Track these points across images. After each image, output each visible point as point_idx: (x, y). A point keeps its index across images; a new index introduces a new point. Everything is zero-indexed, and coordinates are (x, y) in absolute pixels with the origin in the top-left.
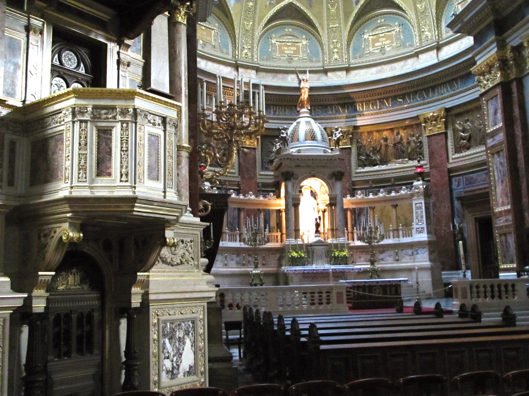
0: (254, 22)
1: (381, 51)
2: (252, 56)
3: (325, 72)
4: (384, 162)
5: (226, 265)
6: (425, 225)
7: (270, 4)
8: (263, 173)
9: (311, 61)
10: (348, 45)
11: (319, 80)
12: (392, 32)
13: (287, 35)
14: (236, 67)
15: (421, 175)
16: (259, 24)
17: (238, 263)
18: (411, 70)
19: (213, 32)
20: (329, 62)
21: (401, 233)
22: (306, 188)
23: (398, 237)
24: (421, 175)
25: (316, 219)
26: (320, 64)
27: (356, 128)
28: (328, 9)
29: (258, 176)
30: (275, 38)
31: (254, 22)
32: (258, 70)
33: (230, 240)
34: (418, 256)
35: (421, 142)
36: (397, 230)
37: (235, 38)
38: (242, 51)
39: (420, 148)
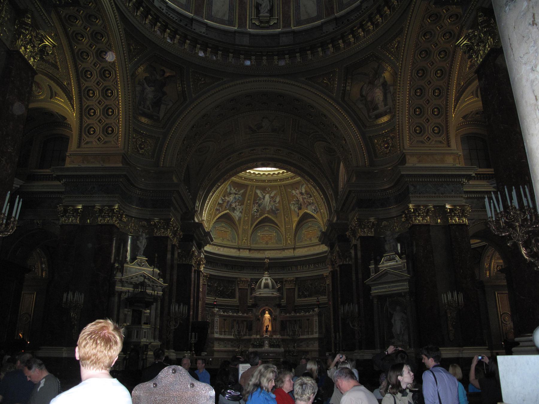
0: (248, 226)
1: (310, 239)
2: (248, 243)
3: (284, 249)
4: (310, 296)
5: (225, 347)
6: (318, 330)
7: (256, 217)
8: (251, 301)
9: (277, 243)
10: (295, 236)
11: (280, 253)
12: (315, 231)
13: (266, 231)
14: (239, 249)
15: (318, 306)
16: (251, 227)
17: (232, 346)
18: (321, 251)
19: (228, 233)
20: (286, 245)
21: (310, 332)
22: (267, 310)
23: (309, 335)
24: (318, 306)
25: (266, 326)
26: (282, 245)
27: (297, 278)
28: (285, 219)
29: (248, 302)
30: (260, 232)
31: (248, 226)
32: (250, 250)
33: (229, 335)
34: (314, 345)
35: (326, 287)
36: (309, 331)
37: (239, 234)
38: (242, 241)
39: (325, 290)
